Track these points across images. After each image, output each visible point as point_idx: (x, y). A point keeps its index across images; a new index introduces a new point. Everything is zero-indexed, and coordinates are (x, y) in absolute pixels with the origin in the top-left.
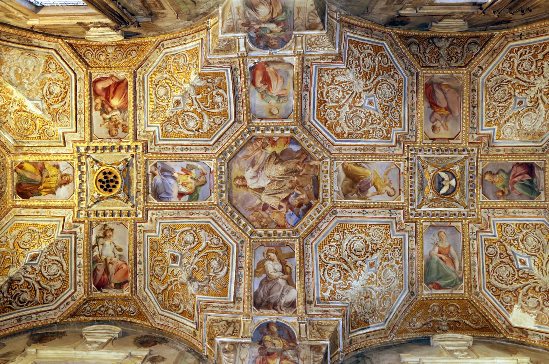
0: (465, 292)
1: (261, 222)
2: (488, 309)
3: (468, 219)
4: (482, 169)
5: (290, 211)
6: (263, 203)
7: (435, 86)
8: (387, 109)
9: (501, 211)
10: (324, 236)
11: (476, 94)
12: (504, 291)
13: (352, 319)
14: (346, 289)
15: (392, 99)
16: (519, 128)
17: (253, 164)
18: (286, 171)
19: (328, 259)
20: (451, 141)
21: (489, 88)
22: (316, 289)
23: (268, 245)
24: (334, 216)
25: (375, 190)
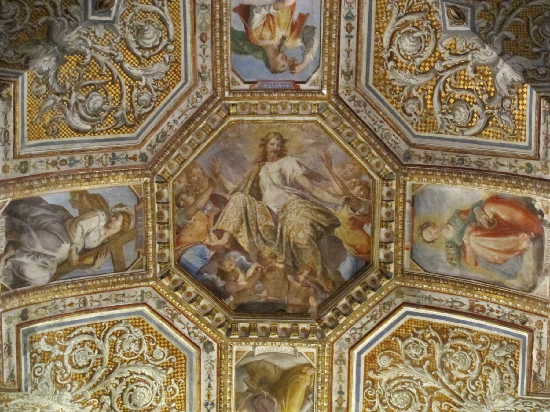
1: (187, 193)
6: (228, 197)
10: (160, 327)
14: (55, 381)
17: (312, 176)
18: (295, 245)
19: (114, 338)
22: (51, 322)
23: (137, 213)
24: (201, 346)
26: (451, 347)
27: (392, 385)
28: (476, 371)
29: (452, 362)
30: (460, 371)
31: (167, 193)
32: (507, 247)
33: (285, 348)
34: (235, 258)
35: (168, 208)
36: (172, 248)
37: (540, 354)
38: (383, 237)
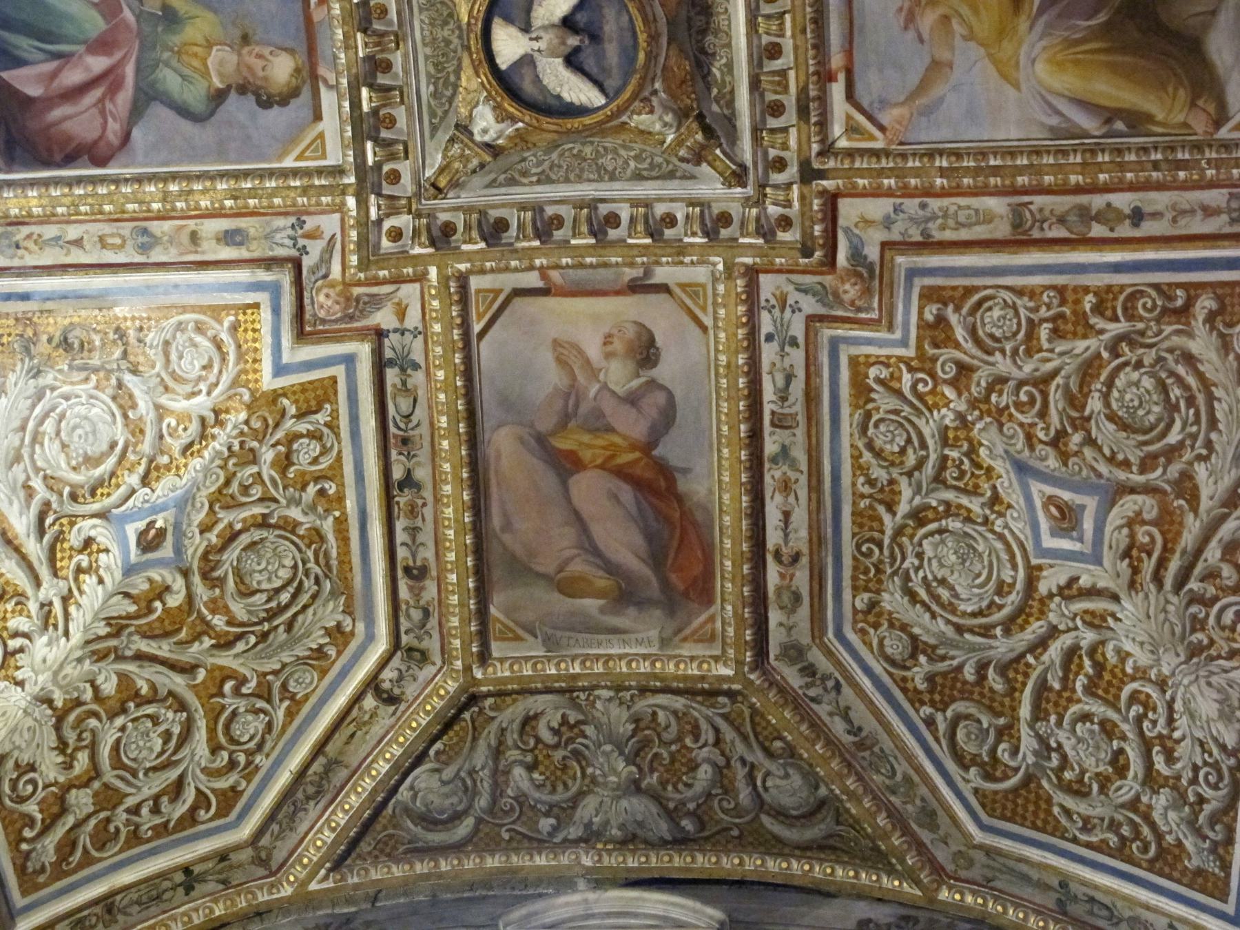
4: (318, 117)
7: (654, 589)
8: (950, 474)
11: (402, 553)
15: (922, 523)
16: (128, 378)
20: (532, 280)
21: (334, 594)
27: (1181, 370)
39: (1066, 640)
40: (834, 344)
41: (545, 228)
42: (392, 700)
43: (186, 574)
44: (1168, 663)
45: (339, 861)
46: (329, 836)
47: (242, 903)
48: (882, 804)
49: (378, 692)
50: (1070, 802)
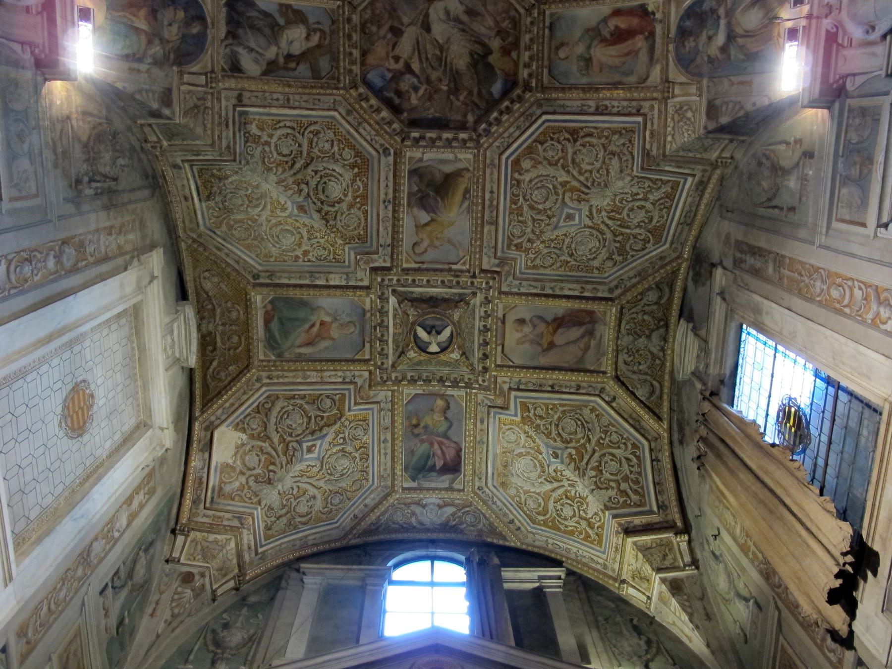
0: (262, 361)
1: (371, 23)
2: (237, 395)
3: (375, 369)
4: (453, 396)
5: (389, 75)
6: (403, 28)
7: (589, 326)
9: (388, 421)
10: (348, 132)
11: (572, 391)
12: (265, 420)
13: (215, 171)
14: (264, 162)
15: (573, 254)
16: (515, 453)
18: (457, 72)
20: (499, 348)
21: (581, 409)
22: (261, 110)
23: (333, 32)
24: (381, 151)
25: (423, 222)
26: (581, 145)
28: (600, 162)
29: (581, 157)
30: (588, 164)
31: (356, 18)
32: (626, 51)
33: (448, 155)
34: (409, 80)
35: (356, 31)
36: (359, 65)
37: (652, 133)
38: (527, 59)
39: (606, 219)
40: (521, 273)
41: (486, 343)
42: (614, 399)
43: (567, 448)
44: (608, 193)
45: (660, 419)
46: (651, 421)
47: (666, 447)
48: (658, 271)
49: (611, 402)
50: (655, 221)
